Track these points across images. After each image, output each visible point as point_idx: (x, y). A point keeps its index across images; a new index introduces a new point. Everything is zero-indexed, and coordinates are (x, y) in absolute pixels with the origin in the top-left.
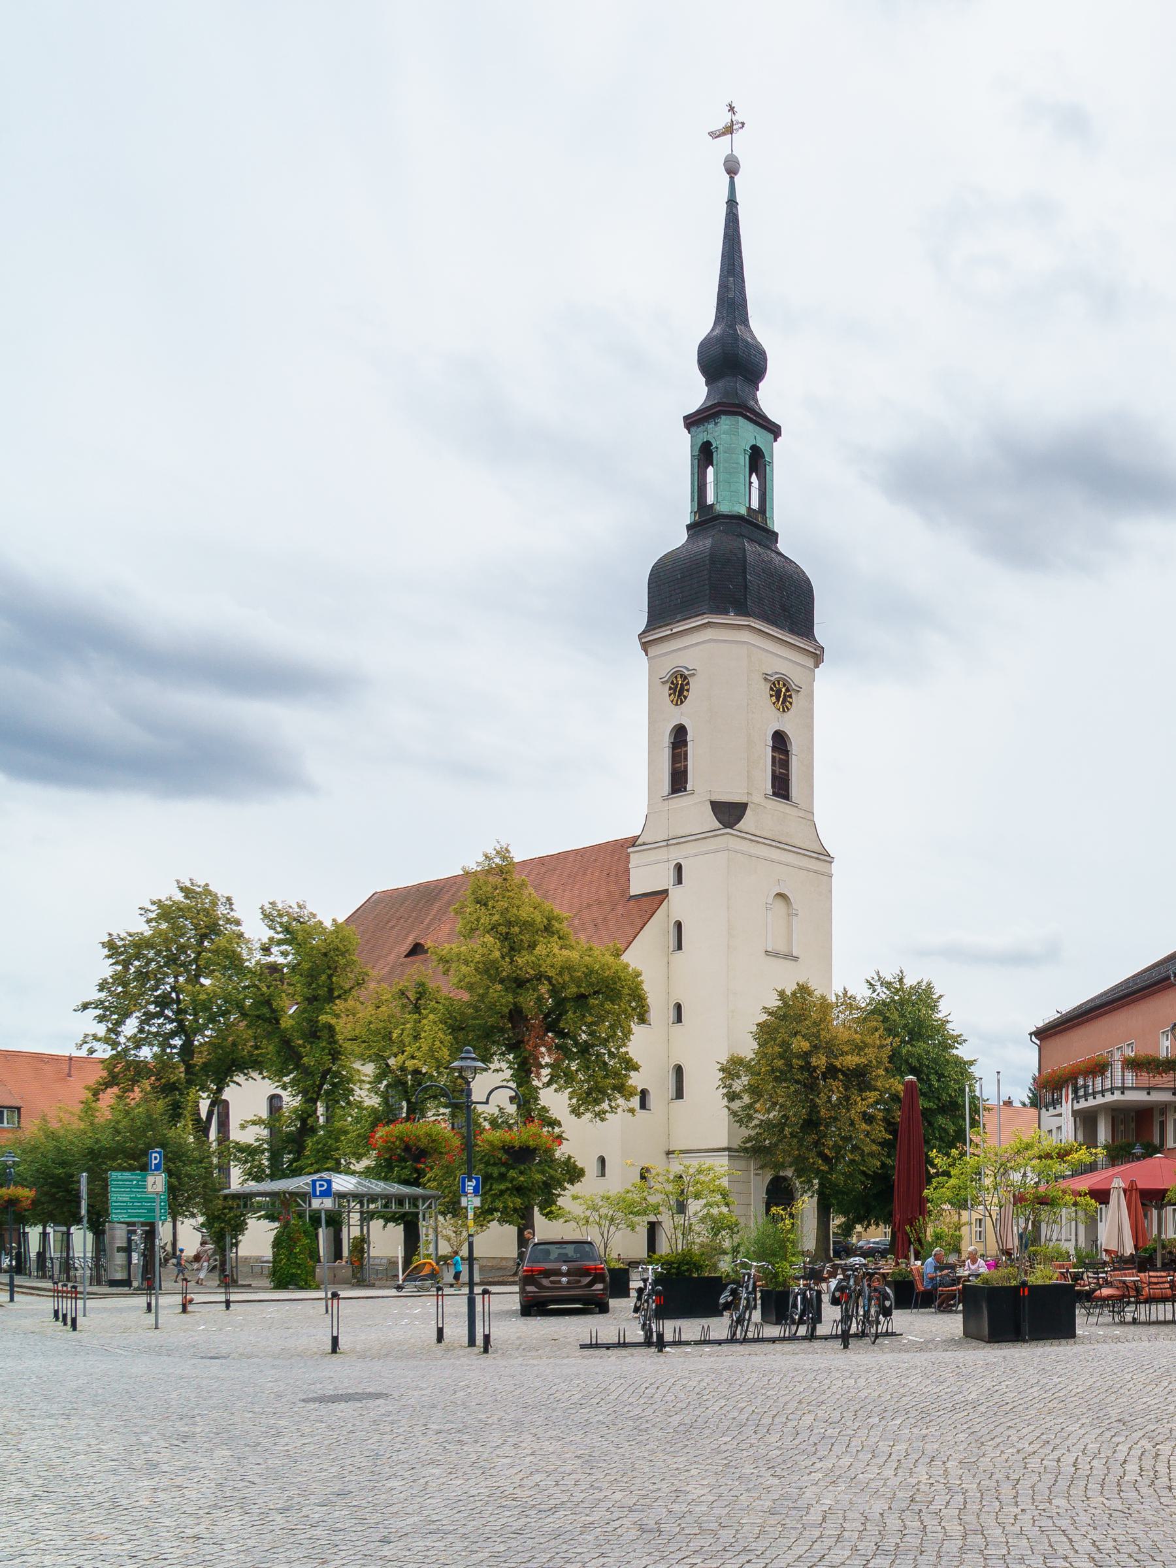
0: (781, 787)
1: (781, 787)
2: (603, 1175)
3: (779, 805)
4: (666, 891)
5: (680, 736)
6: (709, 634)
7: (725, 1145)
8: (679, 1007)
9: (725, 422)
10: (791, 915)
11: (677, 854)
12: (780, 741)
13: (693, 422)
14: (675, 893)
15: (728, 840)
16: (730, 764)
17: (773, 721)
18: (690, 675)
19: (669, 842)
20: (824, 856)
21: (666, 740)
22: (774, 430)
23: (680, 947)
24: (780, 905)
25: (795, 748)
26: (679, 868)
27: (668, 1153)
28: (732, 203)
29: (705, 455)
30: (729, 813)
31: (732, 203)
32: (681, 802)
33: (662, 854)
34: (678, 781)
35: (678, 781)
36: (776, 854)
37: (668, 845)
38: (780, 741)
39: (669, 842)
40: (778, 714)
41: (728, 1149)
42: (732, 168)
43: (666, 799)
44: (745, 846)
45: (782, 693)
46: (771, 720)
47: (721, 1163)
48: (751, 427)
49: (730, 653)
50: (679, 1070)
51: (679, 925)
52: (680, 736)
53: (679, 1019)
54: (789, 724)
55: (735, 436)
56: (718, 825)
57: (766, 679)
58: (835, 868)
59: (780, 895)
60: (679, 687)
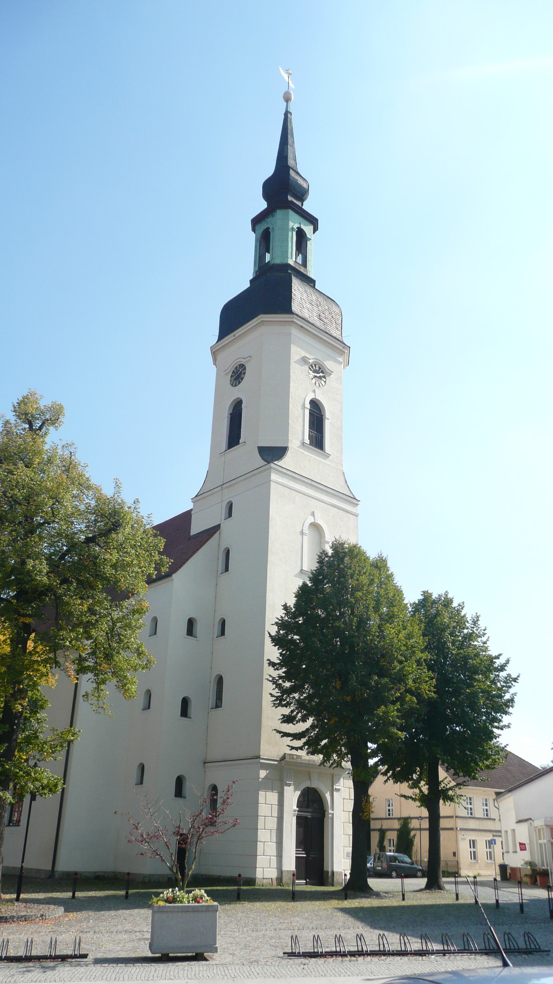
2: (141, 783)
9: (279, 213)
13: (256, 222)
14: (227, 526)
23: (227, 569)
28: (287, 114)
31: (287, 114)
35: (234, 438)
42: (287, 99)
50: (220, 681)
53: (223, 633)
60: (238, 375)
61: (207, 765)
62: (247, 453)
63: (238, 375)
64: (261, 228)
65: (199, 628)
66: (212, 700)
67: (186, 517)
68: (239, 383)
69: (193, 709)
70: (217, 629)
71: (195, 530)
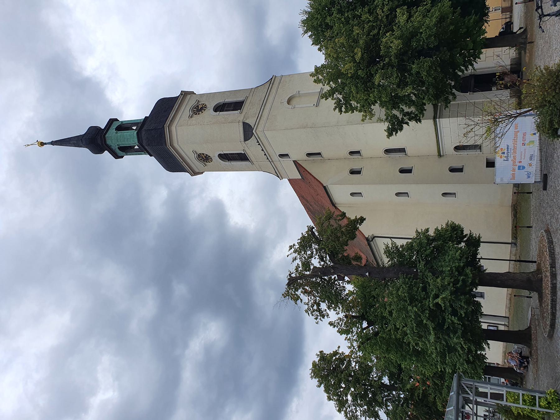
0: (237, 106)
1: (237, 106)
3: (246, 107)
4: (295, 162)
5: (225, 157)
6: (176, 145)
7: (431, 122)
8: (352, 153)
10: (299, 95)
11: (276, 158)
12: (220, 108)
13: (117, 156)
14: (294, 157)
15: (258, 131)
16: (225, 133)
17: (209, 113)
18: (197, 153)
19: (271, 162)
20: (271, 81)
21: (228, 163)
22: (112, 121)
23: (319, 154)
24: (294, 102)
25: (221, 100)
26: (282, 156)
27: (440, 155)
28: (53, 143)
29: (127, 150)
30: (248, 132)
31: (53, 143)
32: (250, 154)
33: (278, 164)
34: (242, 157)
36: (268, 106)
37: (273, 161)
38: (220, 108)
39: (271, 162)
40: (206, 110)
41: (435, 118)
42: (42, 144)
43: (252, 163)
44: (262, 122)
45: (198, 109)
46: (209, 113)
47: (444, 122)
48: (110, 131)
49: (184, 134)
51: (309, 155)
52: (225, 157)
53: (358, 152)
54: (211, 105)
55: (113, 138)
56: (253, 137)
57: (191, 117)
58: (278, 75)
59: (289, 102)
60: (205, 158)
61: (442, 154)
62: (251, 148)
63: (205, 158)
64: (120, 153)
65: (356, 167)
66: (401, 155)
67: (291, 181)
68: (209, 157)
69: (406, 166)
70: (356, 156)
71: (298, 176)
